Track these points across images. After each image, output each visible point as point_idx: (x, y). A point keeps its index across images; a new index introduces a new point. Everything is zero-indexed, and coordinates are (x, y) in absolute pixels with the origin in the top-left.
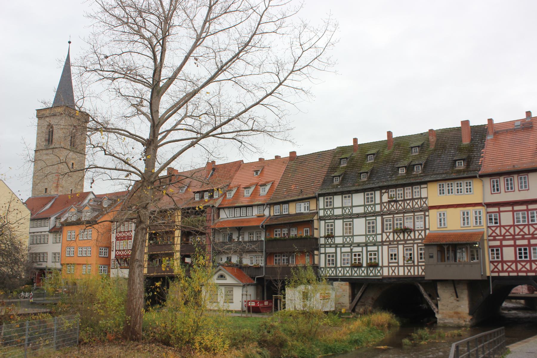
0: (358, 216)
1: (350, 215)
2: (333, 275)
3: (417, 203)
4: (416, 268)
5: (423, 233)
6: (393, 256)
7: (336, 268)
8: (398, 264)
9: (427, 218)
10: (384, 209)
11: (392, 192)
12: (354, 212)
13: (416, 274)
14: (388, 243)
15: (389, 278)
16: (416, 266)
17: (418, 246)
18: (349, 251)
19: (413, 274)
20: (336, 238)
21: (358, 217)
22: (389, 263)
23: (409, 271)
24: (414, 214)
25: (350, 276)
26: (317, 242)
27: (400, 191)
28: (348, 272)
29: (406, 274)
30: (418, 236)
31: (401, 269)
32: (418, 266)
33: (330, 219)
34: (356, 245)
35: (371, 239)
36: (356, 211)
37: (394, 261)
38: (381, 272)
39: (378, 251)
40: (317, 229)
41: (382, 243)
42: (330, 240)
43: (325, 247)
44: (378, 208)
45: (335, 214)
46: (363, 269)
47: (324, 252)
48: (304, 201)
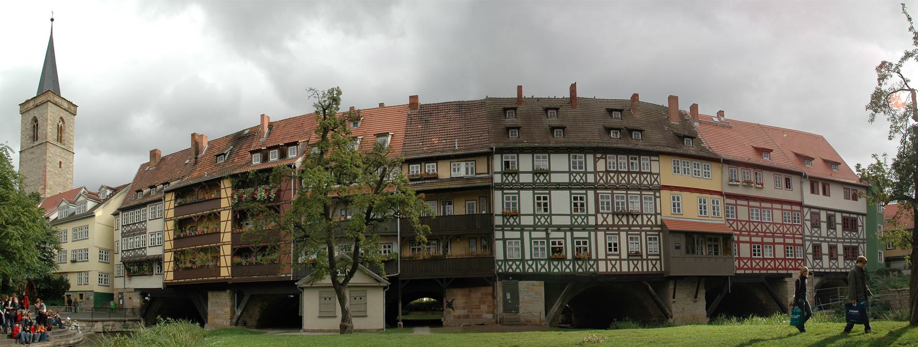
0: (559, 187)
1: (546, 184)
3: (645, 179)
4: (645, 262)
5: (653, 219)
6: (612, 247)
7: (523, 260)
8: (620, 257)
9: (658, 200)
10: (600, 180)
11: (611, 159)
12: (552, 181)
13: (645, 270)
14: (605, 228)
15: (607, 275)
16: (645, 260)
17: (646, 235)
19: (640, 270)
21: (558, 189)
22: (607, 255)
23: (636, 266)
24: (641, 193)
27: (623, 160)
28: (543, 266)
29: (631, 270)
30: (647, 222)
31: (625, 264)
32: (647, 260)
33: (511, 189)
34: (556, 229)
35: (579, 220)
36: (555, 178)
37: (613, 252)
38: (595, 267)
39: (589, 238)
41: (596, 228)
44: (591, 179)
45: (520, 182)
46: (567, 263)
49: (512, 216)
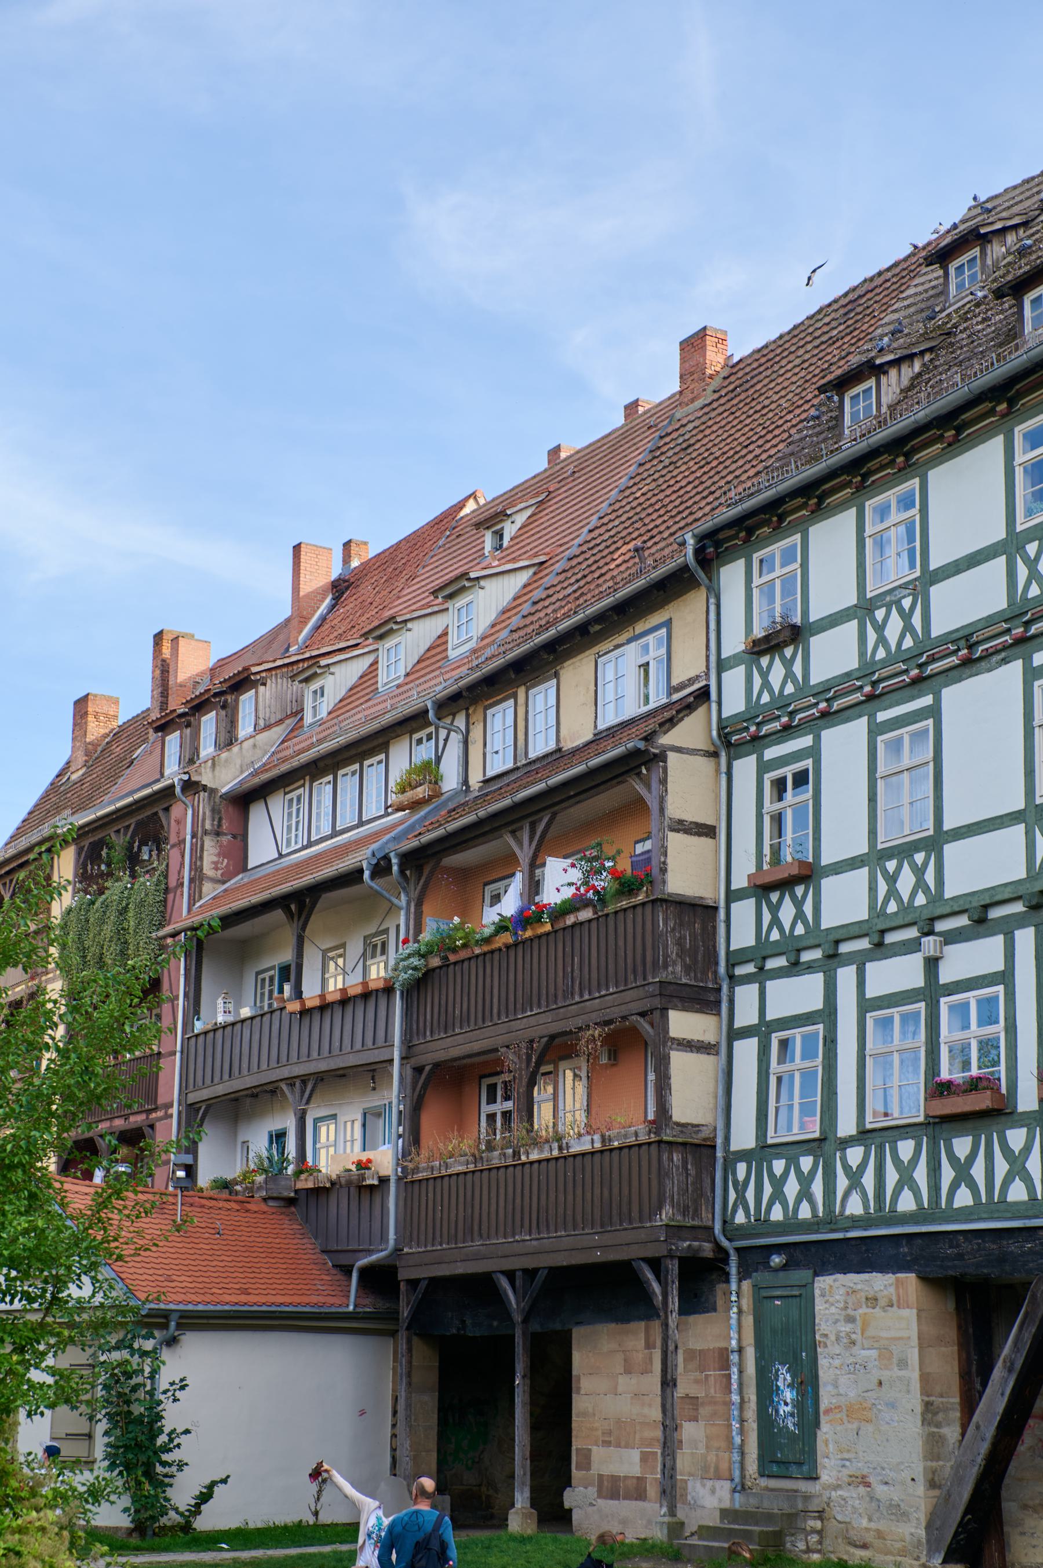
1: (909, 658)
2: (805, 1212)
12: (937, 630)
18: (918, 980)
20: (828, 884)
21: (970, 665)
25: (917, 1216)
26: (711, 934)
33: (788, 731)
34: (963, 921)
40: (707, 831)
42: (787, 912)
43: (762, 976)
47: (754, 1020)
48: (640, 627)
49: (785, 885)
